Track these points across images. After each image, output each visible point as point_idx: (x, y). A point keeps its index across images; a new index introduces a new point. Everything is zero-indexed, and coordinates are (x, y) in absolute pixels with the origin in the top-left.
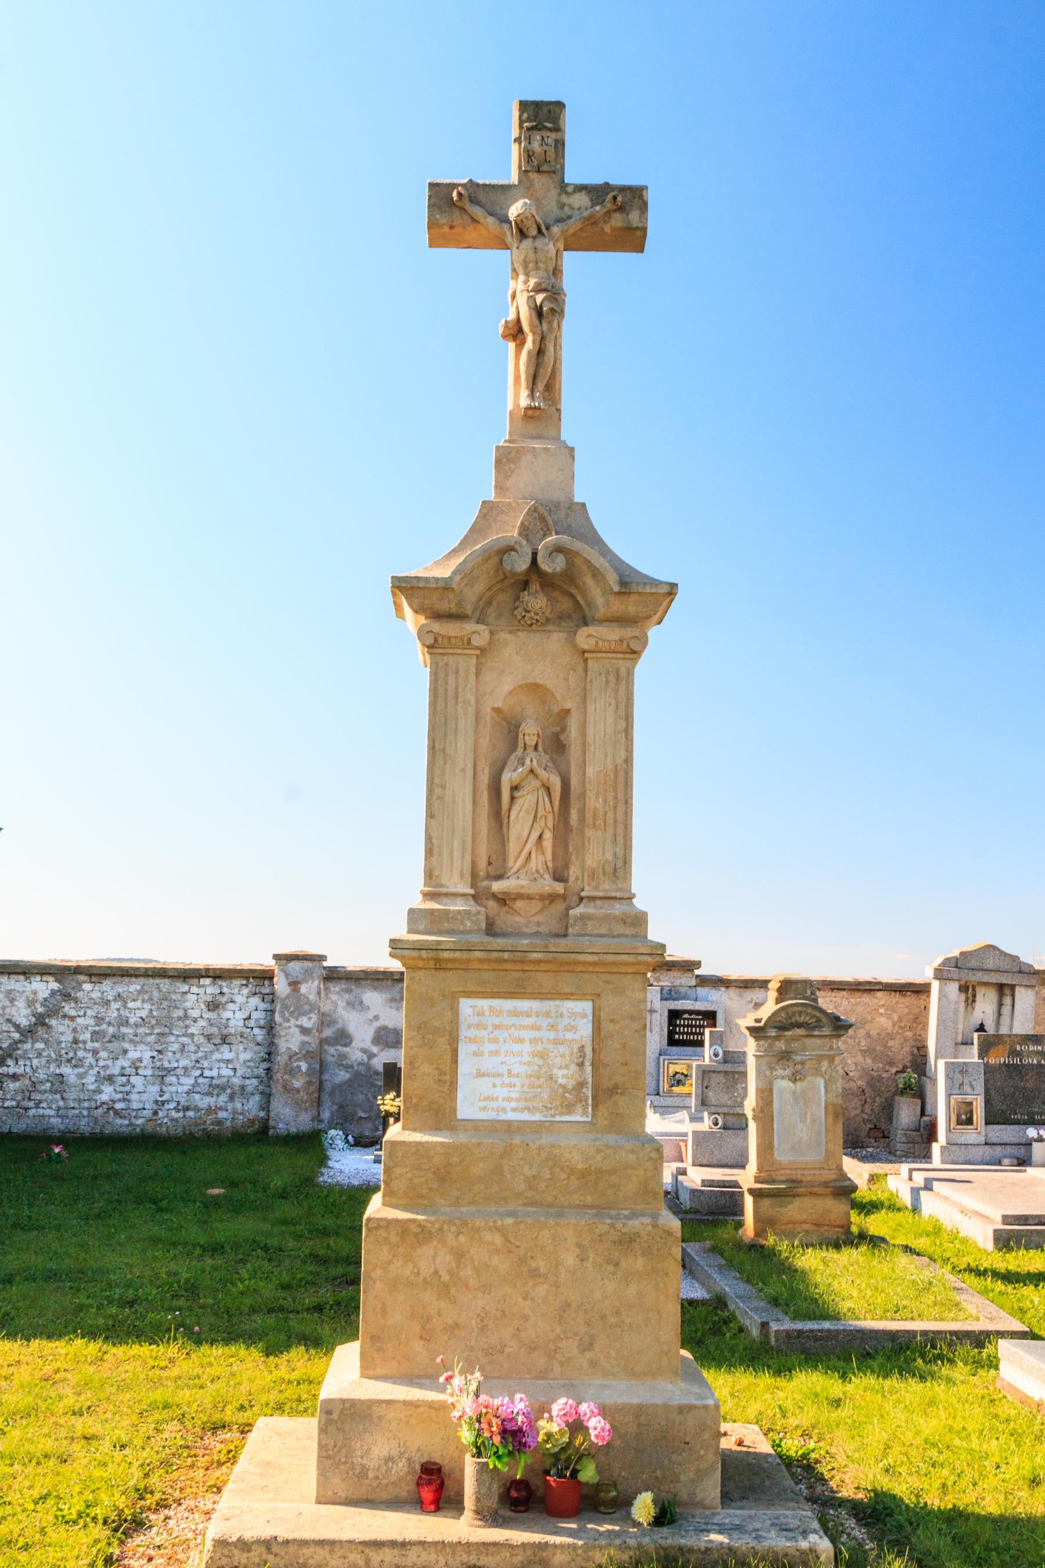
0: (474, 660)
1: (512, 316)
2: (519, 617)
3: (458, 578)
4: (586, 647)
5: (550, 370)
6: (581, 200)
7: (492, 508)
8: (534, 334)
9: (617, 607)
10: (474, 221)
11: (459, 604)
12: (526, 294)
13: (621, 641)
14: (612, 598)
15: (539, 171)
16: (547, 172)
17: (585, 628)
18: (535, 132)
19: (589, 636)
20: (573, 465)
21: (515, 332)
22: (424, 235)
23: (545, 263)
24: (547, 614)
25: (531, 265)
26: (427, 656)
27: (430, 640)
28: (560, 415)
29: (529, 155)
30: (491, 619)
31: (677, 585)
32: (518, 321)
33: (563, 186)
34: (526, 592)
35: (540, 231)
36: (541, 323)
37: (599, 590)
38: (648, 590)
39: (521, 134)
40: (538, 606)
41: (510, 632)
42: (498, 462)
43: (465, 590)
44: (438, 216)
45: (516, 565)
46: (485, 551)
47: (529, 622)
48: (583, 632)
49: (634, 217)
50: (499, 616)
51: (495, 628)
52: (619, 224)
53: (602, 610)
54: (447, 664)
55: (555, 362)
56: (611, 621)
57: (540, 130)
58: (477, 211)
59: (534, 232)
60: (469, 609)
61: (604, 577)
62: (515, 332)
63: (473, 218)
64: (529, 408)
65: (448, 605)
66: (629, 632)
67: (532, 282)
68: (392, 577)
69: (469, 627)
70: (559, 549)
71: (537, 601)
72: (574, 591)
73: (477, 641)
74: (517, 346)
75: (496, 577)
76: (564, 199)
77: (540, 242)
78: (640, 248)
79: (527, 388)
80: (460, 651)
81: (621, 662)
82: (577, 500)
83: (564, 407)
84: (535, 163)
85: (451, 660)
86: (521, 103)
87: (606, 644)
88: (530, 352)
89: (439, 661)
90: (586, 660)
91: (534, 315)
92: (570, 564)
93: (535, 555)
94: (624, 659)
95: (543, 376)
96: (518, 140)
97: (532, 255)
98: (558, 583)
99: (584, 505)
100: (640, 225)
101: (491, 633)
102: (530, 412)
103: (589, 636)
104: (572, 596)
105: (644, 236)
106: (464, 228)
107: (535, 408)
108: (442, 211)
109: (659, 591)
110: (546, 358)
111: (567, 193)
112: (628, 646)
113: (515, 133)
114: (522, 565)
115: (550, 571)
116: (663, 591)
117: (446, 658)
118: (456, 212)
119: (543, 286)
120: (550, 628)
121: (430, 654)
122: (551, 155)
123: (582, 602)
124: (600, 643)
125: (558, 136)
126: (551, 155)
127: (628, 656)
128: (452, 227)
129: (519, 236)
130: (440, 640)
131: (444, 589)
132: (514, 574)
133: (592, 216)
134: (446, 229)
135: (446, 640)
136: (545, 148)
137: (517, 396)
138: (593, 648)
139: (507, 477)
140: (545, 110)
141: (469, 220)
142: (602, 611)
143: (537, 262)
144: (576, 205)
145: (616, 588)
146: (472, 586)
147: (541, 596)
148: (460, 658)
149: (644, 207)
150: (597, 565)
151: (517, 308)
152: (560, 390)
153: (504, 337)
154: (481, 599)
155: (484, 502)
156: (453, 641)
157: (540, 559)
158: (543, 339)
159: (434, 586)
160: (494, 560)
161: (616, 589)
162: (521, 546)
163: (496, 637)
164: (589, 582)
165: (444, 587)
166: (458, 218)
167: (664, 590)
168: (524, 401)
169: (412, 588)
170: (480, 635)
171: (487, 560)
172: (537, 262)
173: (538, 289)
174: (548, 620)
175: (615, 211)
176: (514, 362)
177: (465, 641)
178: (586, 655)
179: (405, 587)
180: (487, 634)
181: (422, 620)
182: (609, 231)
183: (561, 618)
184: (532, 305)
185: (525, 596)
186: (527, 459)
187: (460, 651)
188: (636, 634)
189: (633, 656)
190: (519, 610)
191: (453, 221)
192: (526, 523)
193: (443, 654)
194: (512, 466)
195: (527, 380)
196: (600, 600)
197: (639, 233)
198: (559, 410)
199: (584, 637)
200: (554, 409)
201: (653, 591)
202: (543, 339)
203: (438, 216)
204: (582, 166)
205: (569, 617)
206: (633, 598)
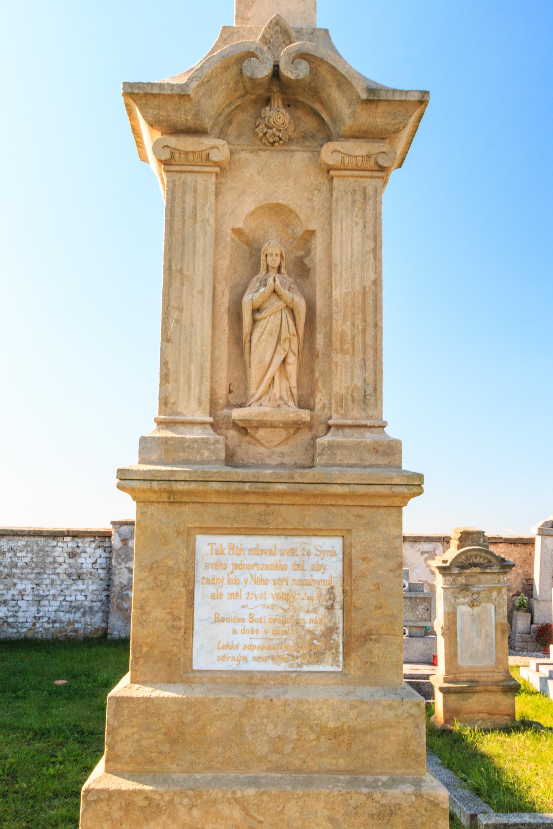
0: (213, 179)
2: (261, 135)
3: (194, 84)
4: (331, 162)
7: (233, 34)
9: (367, 118)
11: (196, 115)
13: (369, 156)
14: (358, 108)
17: (329, 143)
19: (336, 151)
24: (290, 134)
26: (164, 174)
27: (166, 155)
30: (231, 138)
34: (268, 108)
37: (345, 101)
38: (397, 97)
40: (280, 122)
41: (251, 152)
43: (203, 100)
45: (257, 72)
47: (271, 140)
50: (239, 136)
53: (348, 122)
54: (184, 183)
56: (357, 138)
60: (207, 123)
61: (351, 85)
65: (183, 117)
66: (375, 147)
68: (124, 83)
69: (206, 142)
70: (303, 56)
71: (278, 115)
72: (317, 107)
73: (215, 156)
75: (236, 90)
80: (197, 169)
81: (368, 181)
82: (320, 24)
85: (189, 178)
87: (353, 160)
89: (177, 179)
92: (314, 72)
93: (276, 67)
94: (372, 177)
98: (301, 98)
99: (326, 31)
101: (232, 152)
103: (336, 151)
104: (316, 114)
112: (376, 163)
114: (263, 71)
115: (293, 77)
116: (413, 99)
117: (183, 176)
120: (293, 147)
121: (167, 171)
123: (326, 119)
124: (347, 160)
127: (376, 174)
130: (177, 155)
132: (253, 80)
135: (183, 156)
146: (210, 97)
147: (283, 111)
154: (220, 115)
156: (191, 157)
157: (282, 66)
159: (169, 92)
160: (234, 70)
161: (364, 96)
162: (262, 52)
163: (237, 156)
165: (181, 95)
167: (415, 97)
169: (146, 95)
170: (219, 149)
171: (226, 68)
177: (204, 157)
179: (139, 95)
181: (158, 135)
183: (304, 137)
185: (267, 112)
187: (197, 169)
188: (385, 149)
189: (381, 174)
192: (268, 36)
193: (180, 172)
199: (330, 153)
201: (403, 98)
205: (313, 136)
206: (382, 108)
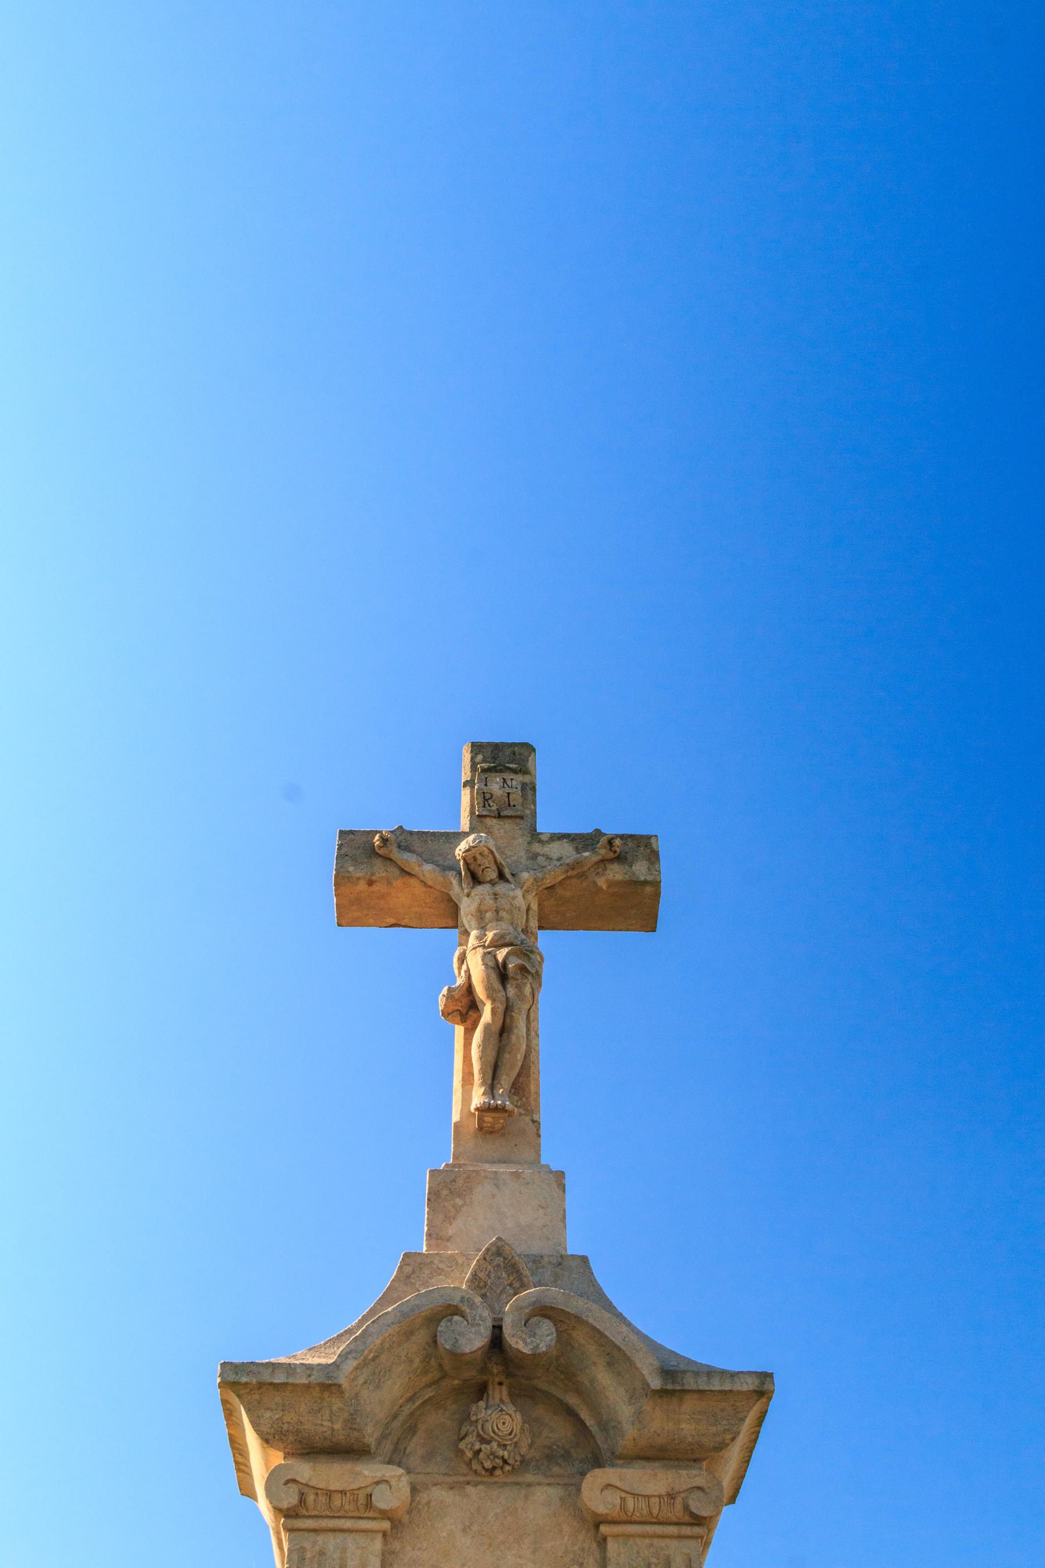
0: (378, 1545)
1: (460, 981)
2: (469, 1454)
3: (351, 1364)
4: (602, 1510)
5: (520, 1057)
6: (564, 850)
7: (421, 1266)
8: (494, 1001)
9: (661, 1423)
10: (405, 873)
11: (351, 1422)
12: (480, 951)
13: (671, 1496)
14: (647, 1406)
15: (499, 816)
16: (510, 817)
17: (597, 1472)
18: (493, 774)
19: (609, 1486)
20: (564, 1200)
21: (465, 1006)
22: (326, 899)
23: (510, 912)
24: (524, 1451)
25: (488, 915)
26: (283, 1535)
27: (290, 1499)
28: (538, 1129)
29: (485, 798)
30: (414, 1461)
31: (771, 1375)
32: (469, 988)
33: (534, 835)
34: (482, 1404)
35: (501, 876)
36: (505, 988)
37: (621, 1391)
38: (716, 1385)
39: (473, 776)
40: (505, 1430)
41: (451, 1488)
42: (434, 1197)
43: (365, 1393)
44: (351, 869)
45: (462, 1341)
46: (404, 1315)
47: (488, 1465)
48: (594, 1480)
49: (640, 869)
50: (429, 1457)
51: (421, 1478)
52: (619, 877)
53: (630, 1431)
54: (322, 1553)
55: (526, 1056)
56: (648, 1459)
57: (501, 771)
58: (409, 860)
59: (493, 875)
60: (371, 1435)
61: (632, 1364)
62: (465, 1006)
63: (402, 870)
64: (483, 1110)
65: (326, 1424)
66: (685, 1478)
67: (490, 935)
68: (224, 1365)
69: (369, 1471)
70: (544, 1311)
71: (502, 1419)
72: (572, 1400)
73: (384, 1500)
74: (466, 1030)
75: (425, 1372)
76: (537, 847)
77: (501, 888)
78: (649, 922)
79: (483, 1084)
80: (348, 1524)
81: (673, 1544)
82: (574, 1247)
83: (544, 1116)
84: (494, 808)
85: (331, 1543)
86: (473, 745)
87: (643, 1504)
88: (487, 1027)
89: (307, 1545)
90: (602, 1542)
91: (494, 976)
92: (564, 1340)
93: (497, 1329)
94: (680, 1537)
95: (508, 1065)
96: (469, 783)
97: (489, 901)
98: (543, 1386)
99: (584, 1260)
100: (649, 878)
101: (414, 1490)
102: (488, 1118)
103: (609, 1486)
104: (571, 1413)
105: (657, 895)
106: (389, 883)
107: (496, 1109)
108: (355, 860)
109: (737, 1387)
110: (514, 1038)
111: (540, 841)
112: (686, 1507)
113: (466, 775)
114: (473, 1340)
115: (526, 1350)
116: (745, 1388)
117: (321, 1538)
118: (378, 862)
119: (507, 939)
120: (529, 1478)
121: (290, 1530)
122: (517, 797)
123: (589, 1422)
124: (630, 1503)
125: (527, 779)
126: (517, 797)
127: (687, 1530)
128: (371, 883)
129: (470, 879)
130: (311, 1498)
131: (325, 1387)
132: (456, 1356)
133: (578, 864)
134: (362, 886)
135: (322, 1499)
136: (508, 790)
137: (466, 1099)
138: (615, 1513)
139: (449, 1219)
140: (508, 752)
141: (398, 872)
142: (630, 1434)
143: (497, 912)
144: (555, 855)
145: (656, 1383)
146: (378, 1387)
147: (510, 1409)
148: (350, 1539)
149: (653, 857)
150: (617, 1340)
151: (468, 971)
152: (537, 1093)
153: (446, 1014)
154: (395, 1417)
155: (407, 1255)
156: (337, 1501)
157: (507, 1332)
158: (508, 1009)
159: (304, 1381)
160: (421, 1337)
161: (656, 1383)
162: (472, 1305)
163: (424, 1497)
164: (604, 1378)
165: (324, 1385)
166: (380, 871)
167: (749, 1385)
168: (478, 1097)
169: (261, 1385)
170: (388, 1483)
171: (409, 1334)
172: (497, 912)
173: (499, 943)
174: (525, 1463)
175: (611, 861)
176: (465, 1050)
177: (362, 1500)
178: (604, 1529)
179: (248, 1386)
180: (406, 1491)
181: (278, 1458)
182: (604, 887)
183: (550, 1458)
184: (491, 964)
185: (480, 1411)
186: (482, 1192)
187: (348, 1524)
188: (700, 1481)
189: (697, 1530)
190: (471, 1439)
191: (372, 874)
192: (482, 1275)
193: (314, 1530)
194: (459, 1202)
195: (483, 1071)
196: (625, 1411)
197: (648, 889)
198: (536, 1123)
199: (600, 1489)
200: (527, 1119)
201: (727, 1387)
202: (508, 1009)
203: (351, 869)
204: (561, 807)
205: (567, 1456)
206: (690, 1404)
